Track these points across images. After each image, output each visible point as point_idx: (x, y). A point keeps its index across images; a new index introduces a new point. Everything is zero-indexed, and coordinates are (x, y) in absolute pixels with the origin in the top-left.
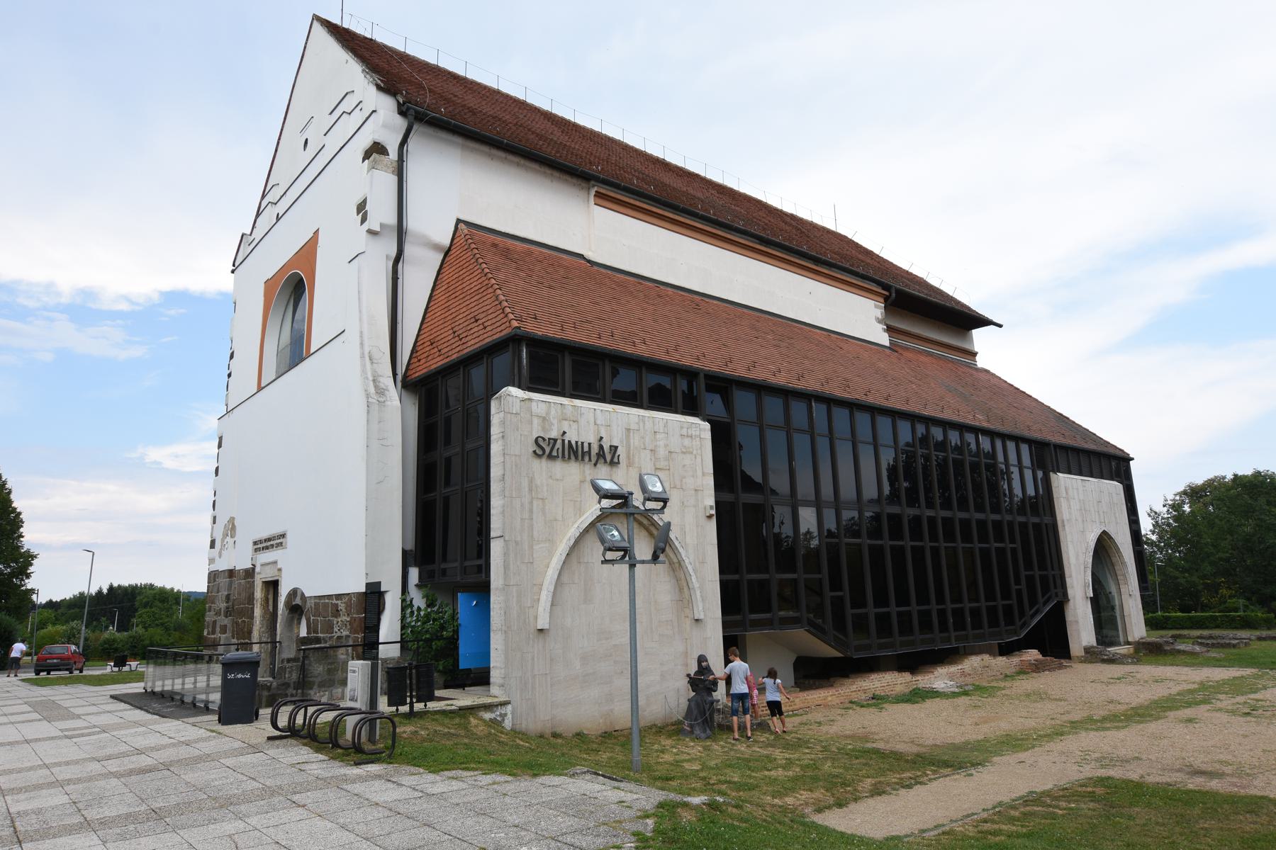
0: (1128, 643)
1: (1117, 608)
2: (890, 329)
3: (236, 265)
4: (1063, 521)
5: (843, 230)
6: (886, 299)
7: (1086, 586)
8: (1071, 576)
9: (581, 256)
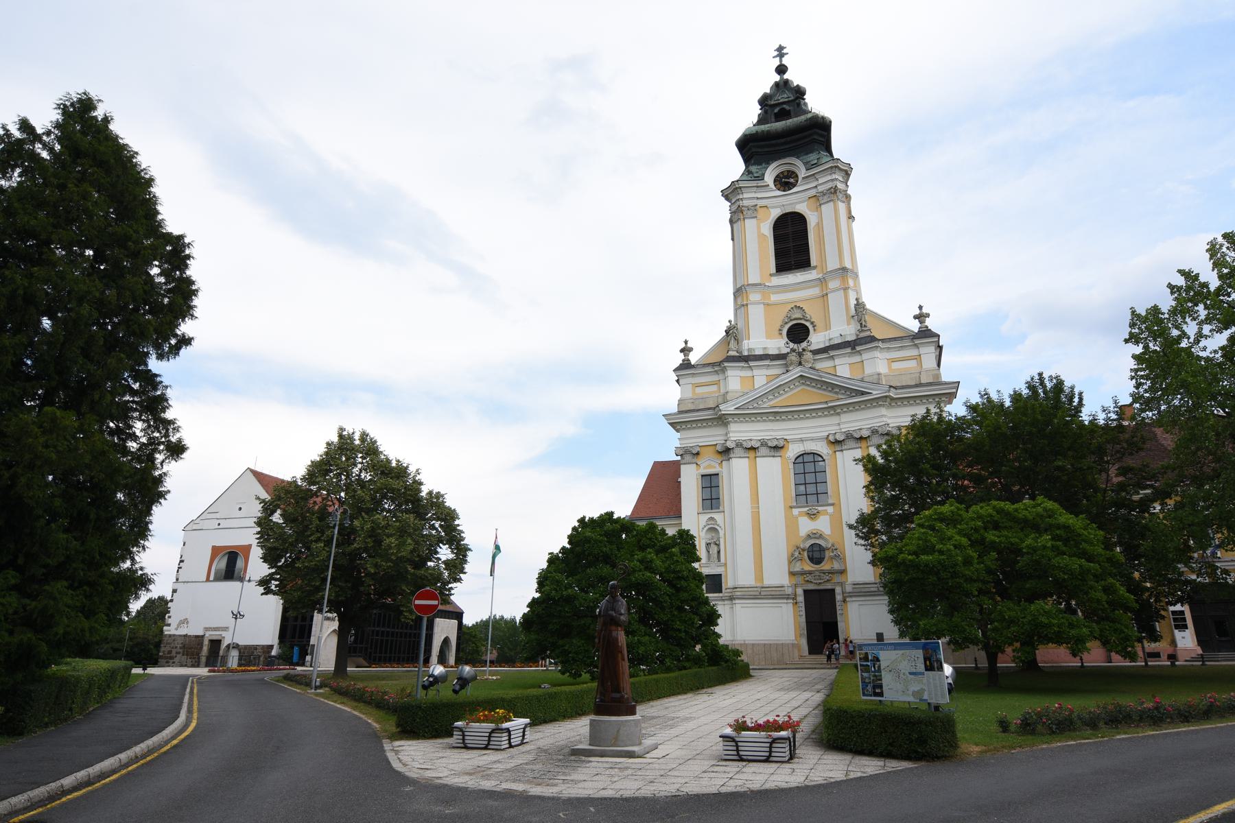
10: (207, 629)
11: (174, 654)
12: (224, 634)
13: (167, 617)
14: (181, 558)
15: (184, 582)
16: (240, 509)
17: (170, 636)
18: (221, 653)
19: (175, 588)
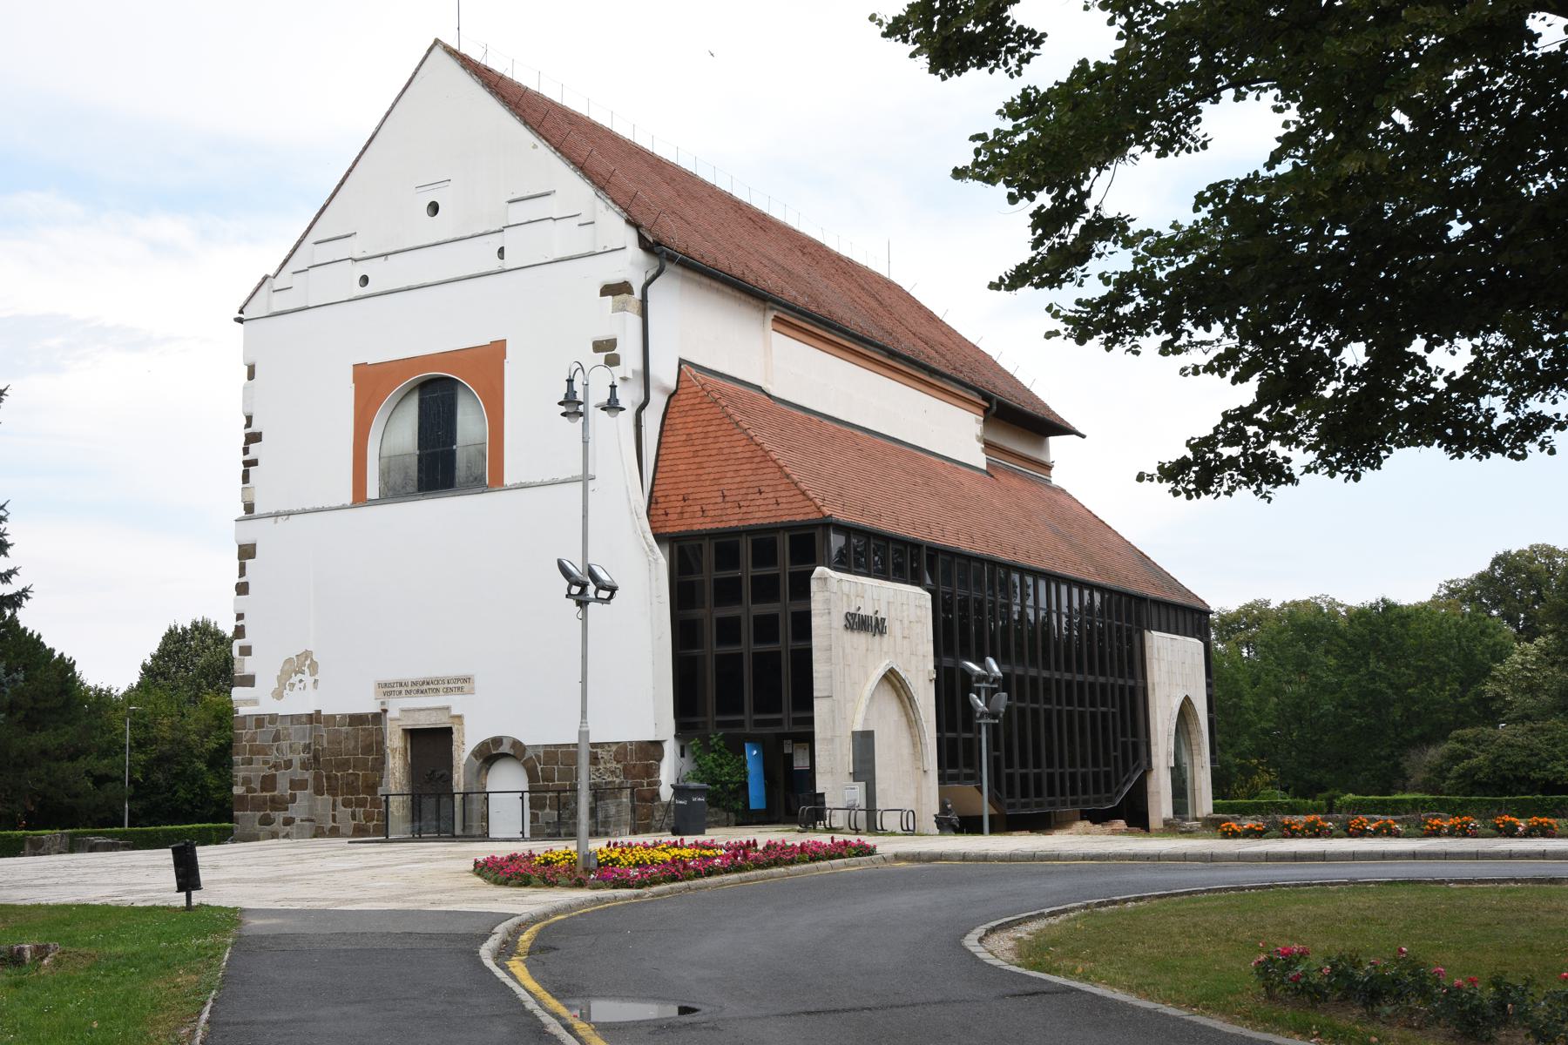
0: (1196, 819)
1: (1189, 781)
2: (989, 446)
4: (1154, 684)
5: (897, 278)
6: (986, 411)
7: (1168, 755)
8: (1156, 744)
9: (759, 388)
10: (388, 689)
11: (283, 788)
12: (457, 703)
13: (236, 652)
14: (248, 425)
15: (270, 516)
16: (434, 208)
17: (260, 720)
18: (459, 781)
19: (247, 540)
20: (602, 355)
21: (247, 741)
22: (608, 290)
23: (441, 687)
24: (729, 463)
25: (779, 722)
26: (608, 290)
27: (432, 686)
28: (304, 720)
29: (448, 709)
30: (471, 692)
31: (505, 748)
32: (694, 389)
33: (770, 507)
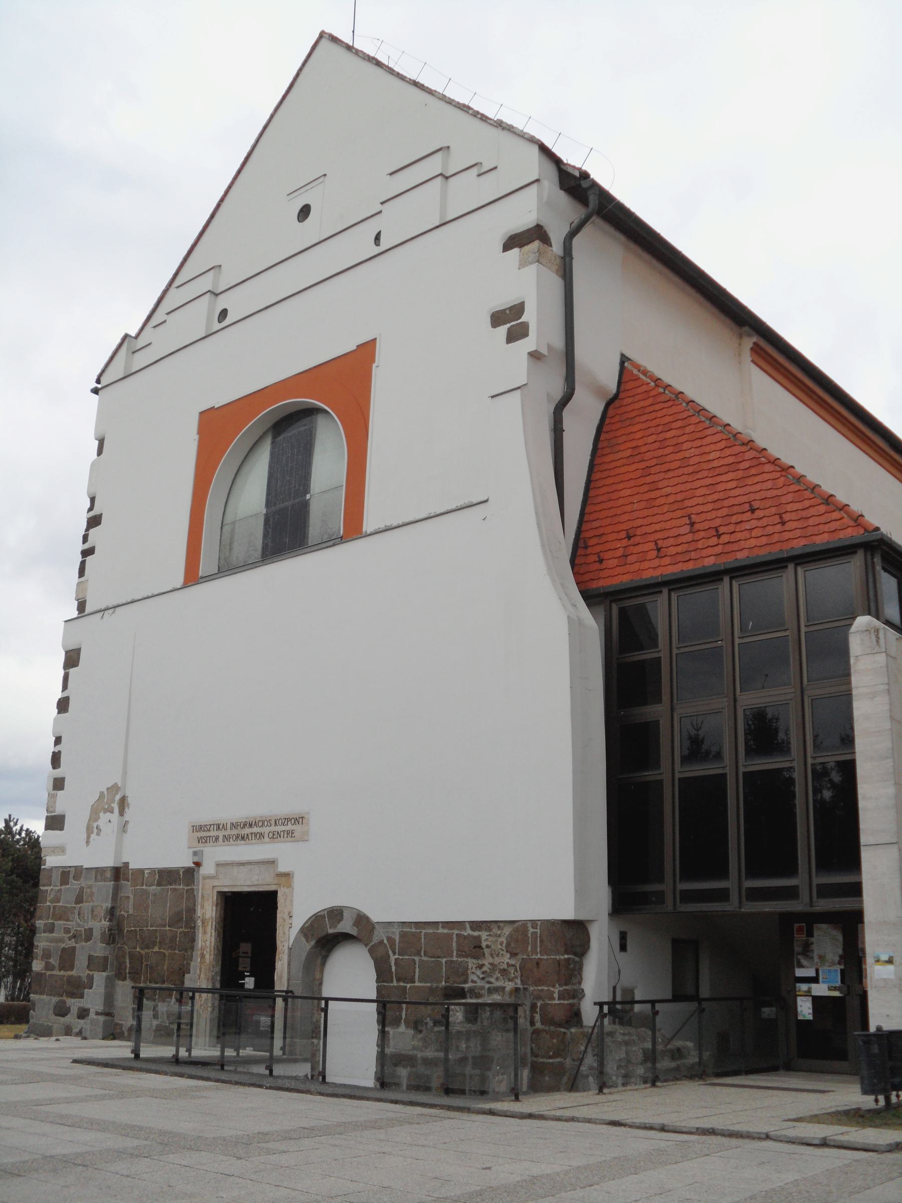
3: (104, 381)
11: (80, 970)
17: (66, 874)
20: (503, 330)
21: (51, 901)
22: (513, 242)
23: (266, 830)
24: (699, 476)
25: (791, 893)
26: (513, 242)
27: (255, 830)
28: (109, 874)
29: (272, 863)
30: (304, 839)
31: (346, 926)
32: (644, 388)
33: (770, 530)
